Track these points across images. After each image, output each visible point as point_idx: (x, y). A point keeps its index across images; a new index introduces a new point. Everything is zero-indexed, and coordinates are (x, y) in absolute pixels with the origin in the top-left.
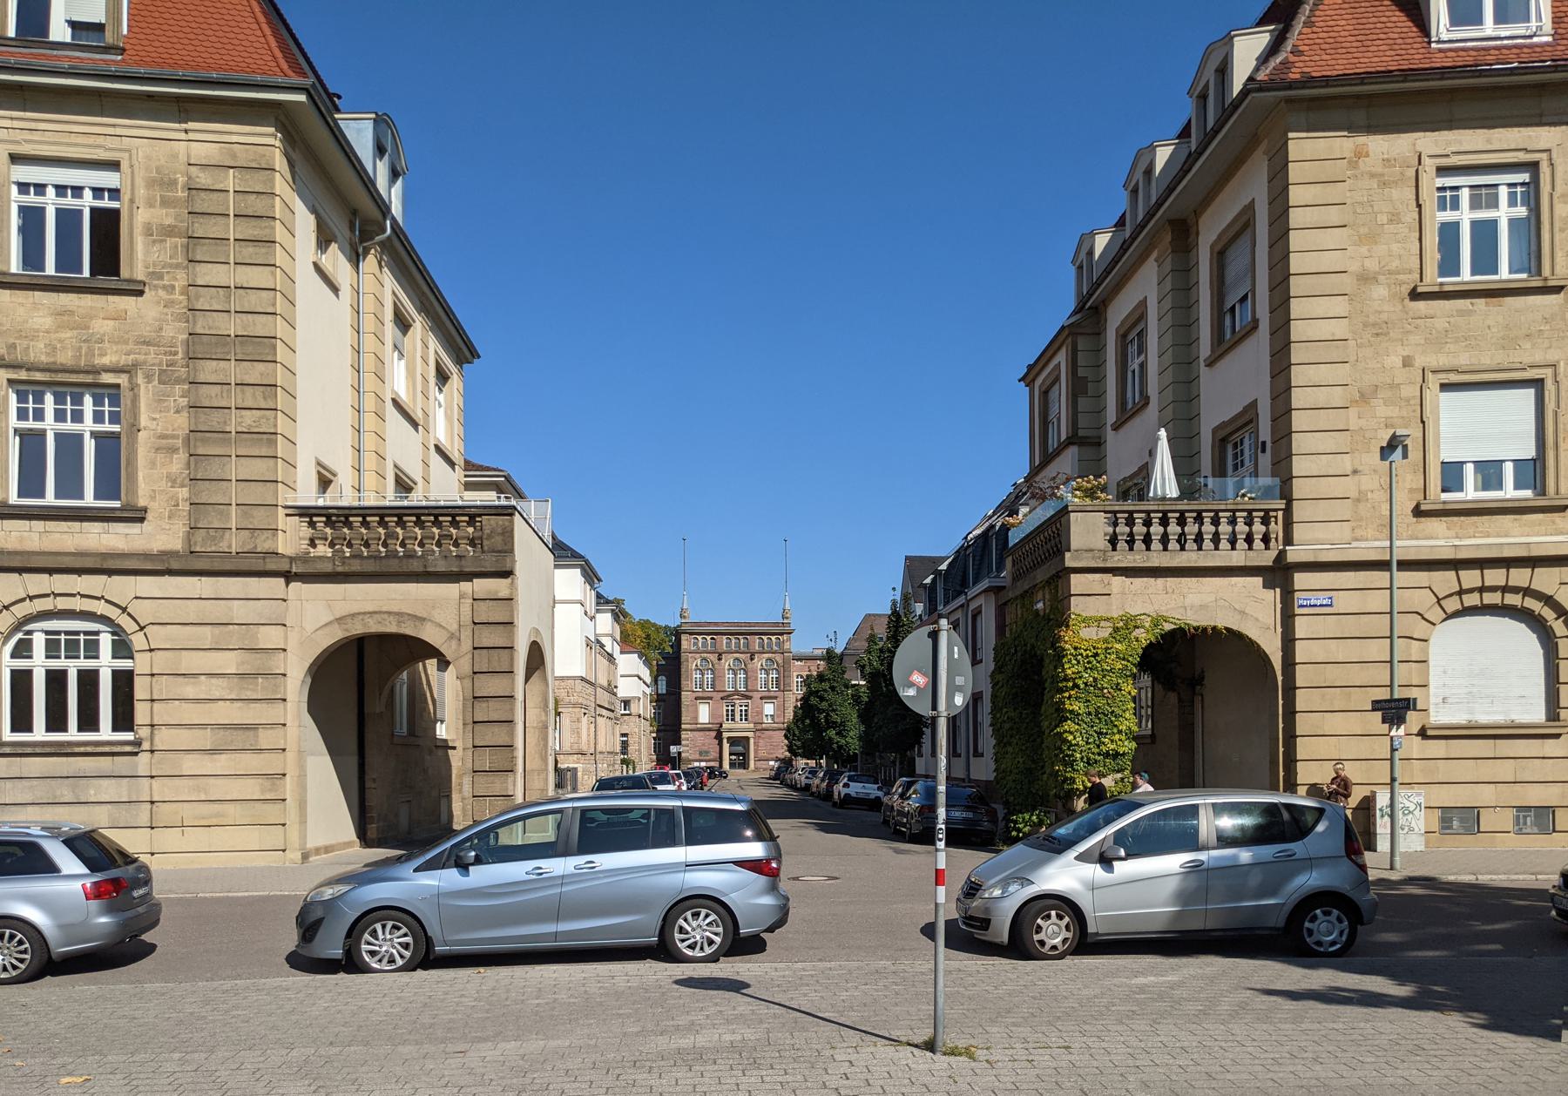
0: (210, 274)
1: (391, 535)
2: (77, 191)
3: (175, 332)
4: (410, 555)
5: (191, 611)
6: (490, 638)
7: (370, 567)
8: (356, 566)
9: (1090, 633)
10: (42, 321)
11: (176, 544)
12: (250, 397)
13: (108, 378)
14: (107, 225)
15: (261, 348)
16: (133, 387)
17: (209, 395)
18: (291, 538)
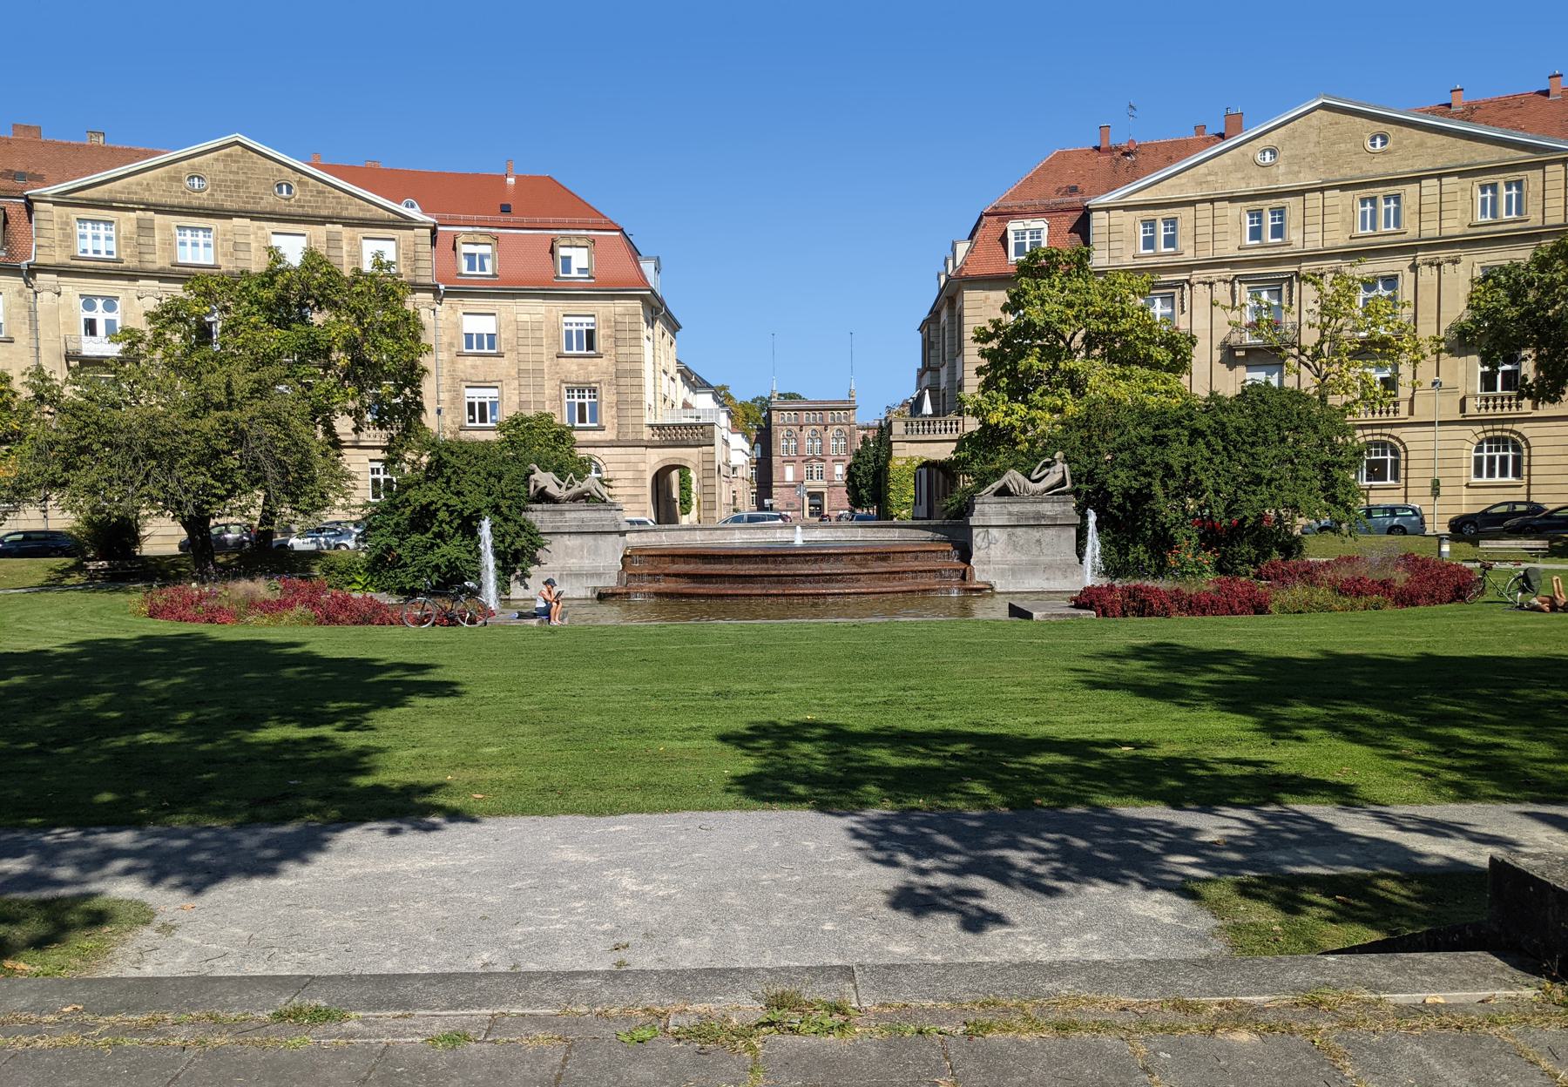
0: (622, 350)
3: (612, 369)
5: (619, 458)
6: (708, 466)
9: (898, 463)
11: (614, 438)
12: (634, 389)
14: (590, 334)
17: (622, 389)
18: (647, 434)
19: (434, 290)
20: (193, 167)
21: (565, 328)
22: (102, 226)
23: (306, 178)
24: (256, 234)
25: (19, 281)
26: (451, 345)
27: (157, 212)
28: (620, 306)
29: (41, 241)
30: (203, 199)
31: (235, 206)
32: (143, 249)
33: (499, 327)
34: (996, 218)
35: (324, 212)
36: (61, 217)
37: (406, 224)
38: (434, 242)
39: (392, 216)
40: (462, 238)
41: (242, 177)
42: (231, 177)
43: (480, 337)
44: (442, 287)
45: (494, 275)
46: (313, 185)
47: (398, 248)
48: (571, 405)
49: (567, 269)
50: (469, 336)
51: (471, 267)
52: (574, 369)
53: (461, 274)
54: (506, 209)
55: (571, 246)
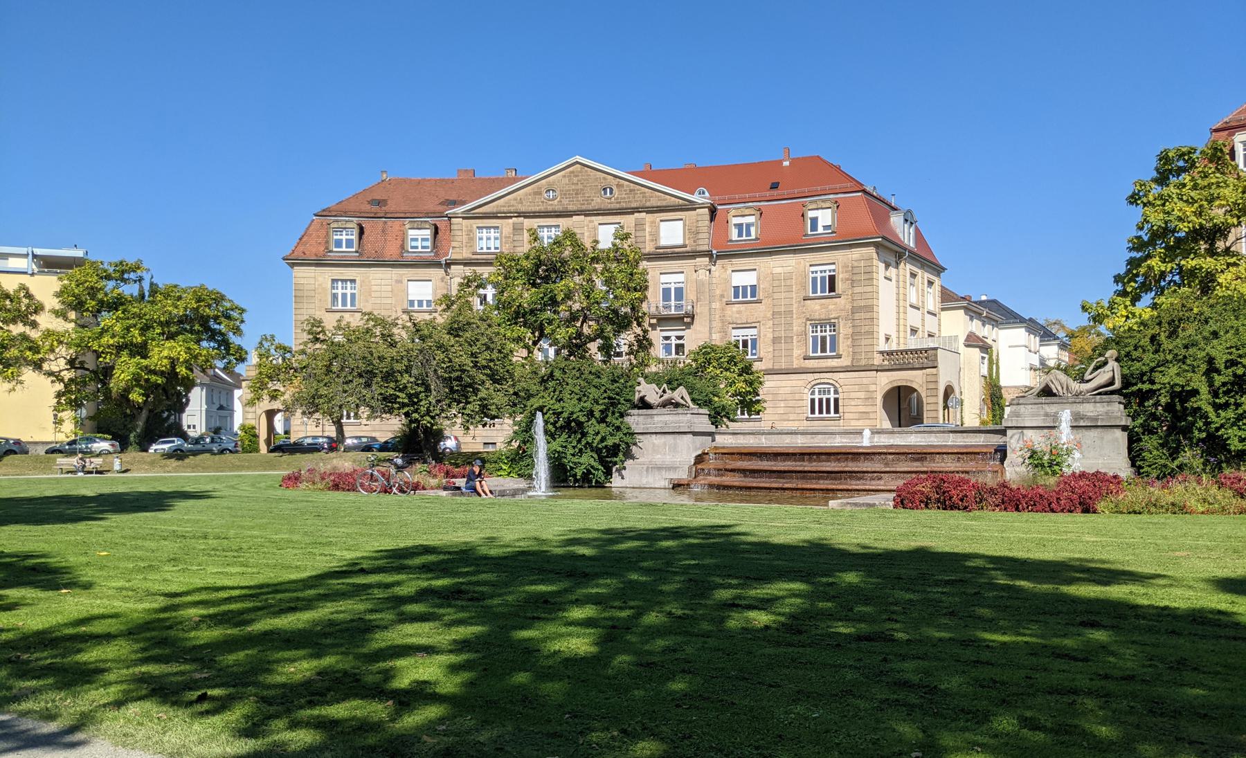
0: (857, 290)
1: (904, 357)
2: (825, 271)
3: (849, 307)
4: (909, 363)
6: (931, 386)
7: (898, 367)
8: (895, 367)
10: (817, 307)
11: (849, 364)
13: (833, 321)
14: (832, 279)
15: (869, 309)
16: (839, 322)
18: (877, 360)
19: (709, 254)
20: (549, 184)
21: (811, 275)
22: (492, 230)
23: (622, 182)
24: (588, 226)
25: (441, 272)
26: (722, 296)
27: (525, 217)
28: (856, 253)
29: (454, 244)
30: (555, 205)
31: (575, 208)
32: (516, 244)
33: (759, 279)
34: (1227, 132)
35: (634, 205)
36: (467, 227)
37: (690, 206)
38: (712, 219)
39: (681, 202)
40: (733, 212)
41: (580, 186)
42: (573, 187)
43: (745, 288)
44: (714, 252)
45: (757, 239)
46: (627, 186)
47: (685, 225)
48: (815, 338)
49: (814, 227)
50: (736, 288)
51: (740, 235)
52: (816, 308)
53: (731, 241)
54: (775, 186)
55: (817, 209)
